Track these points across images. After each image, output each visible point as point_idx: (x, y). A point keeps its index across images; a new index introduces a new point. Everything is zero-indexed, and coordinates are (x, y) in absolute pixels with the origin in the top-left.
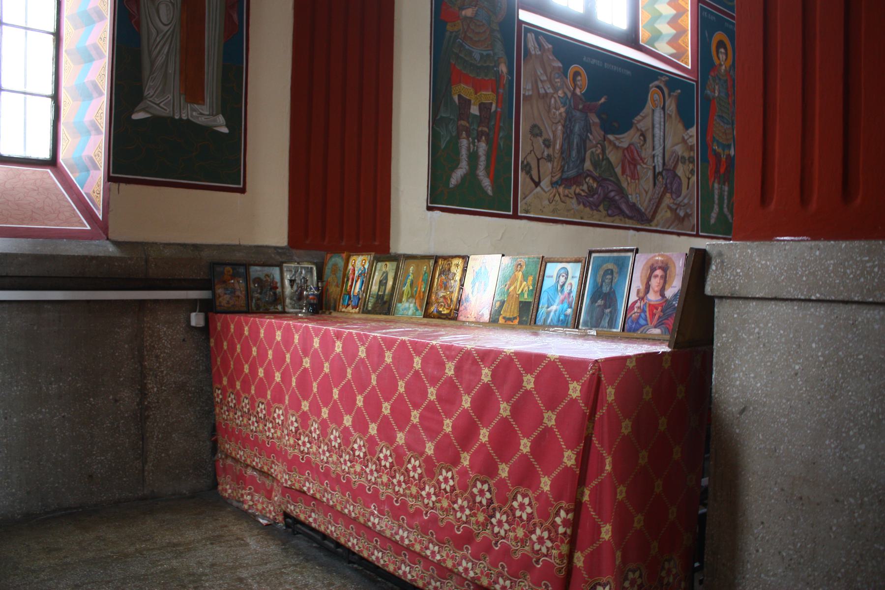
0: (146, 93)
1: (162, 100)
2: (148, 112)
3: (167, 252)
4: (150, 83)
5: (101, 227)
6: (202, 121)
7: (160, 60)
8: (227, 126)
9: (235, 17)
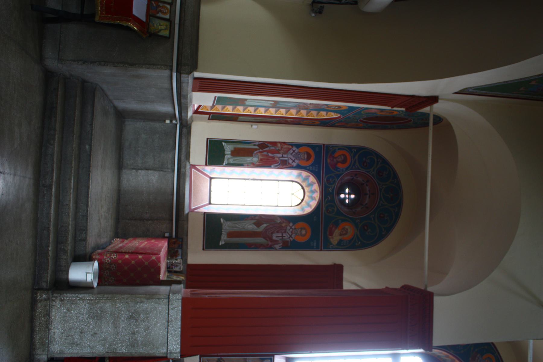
1: (227, 226)
5: (192, 211)
6: (222, 237)
7: (237, 226)
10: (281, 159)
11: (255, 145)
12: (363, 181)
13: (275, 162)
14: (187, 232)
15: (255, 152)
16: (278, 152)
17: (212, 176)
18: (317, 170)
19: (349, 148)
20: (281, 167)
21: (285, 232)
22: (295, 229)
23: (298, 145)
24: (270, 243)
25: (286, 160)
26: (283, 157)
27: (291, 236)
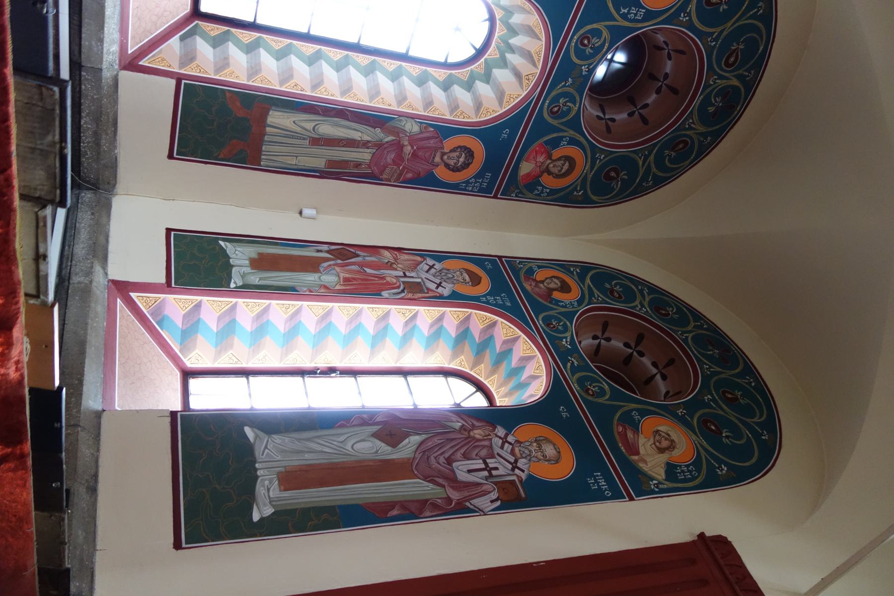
0: (274, 436)
1: (271, 455)
2: (255, 439)
3: (85, 451)
4: (287, 440)
6: (260, 490)
7: (313, 445)
8: (262, 519)
9: (395, 512)
10: (402, 279)
11: (318, 251)
12: (626, 345)
13: (390, 286)
14: (96, 476)
15: (326, 264)
16: (390, 266)
17: (191, 362)
18: (509, 304)
19: (564, 266)
20: (410, 296)
21: (493, 457)
22: (517, 441)
23: (440, 256)
24: (455, 496)
25: (419, 283)
26: (405, 276)
27: (515, 466)
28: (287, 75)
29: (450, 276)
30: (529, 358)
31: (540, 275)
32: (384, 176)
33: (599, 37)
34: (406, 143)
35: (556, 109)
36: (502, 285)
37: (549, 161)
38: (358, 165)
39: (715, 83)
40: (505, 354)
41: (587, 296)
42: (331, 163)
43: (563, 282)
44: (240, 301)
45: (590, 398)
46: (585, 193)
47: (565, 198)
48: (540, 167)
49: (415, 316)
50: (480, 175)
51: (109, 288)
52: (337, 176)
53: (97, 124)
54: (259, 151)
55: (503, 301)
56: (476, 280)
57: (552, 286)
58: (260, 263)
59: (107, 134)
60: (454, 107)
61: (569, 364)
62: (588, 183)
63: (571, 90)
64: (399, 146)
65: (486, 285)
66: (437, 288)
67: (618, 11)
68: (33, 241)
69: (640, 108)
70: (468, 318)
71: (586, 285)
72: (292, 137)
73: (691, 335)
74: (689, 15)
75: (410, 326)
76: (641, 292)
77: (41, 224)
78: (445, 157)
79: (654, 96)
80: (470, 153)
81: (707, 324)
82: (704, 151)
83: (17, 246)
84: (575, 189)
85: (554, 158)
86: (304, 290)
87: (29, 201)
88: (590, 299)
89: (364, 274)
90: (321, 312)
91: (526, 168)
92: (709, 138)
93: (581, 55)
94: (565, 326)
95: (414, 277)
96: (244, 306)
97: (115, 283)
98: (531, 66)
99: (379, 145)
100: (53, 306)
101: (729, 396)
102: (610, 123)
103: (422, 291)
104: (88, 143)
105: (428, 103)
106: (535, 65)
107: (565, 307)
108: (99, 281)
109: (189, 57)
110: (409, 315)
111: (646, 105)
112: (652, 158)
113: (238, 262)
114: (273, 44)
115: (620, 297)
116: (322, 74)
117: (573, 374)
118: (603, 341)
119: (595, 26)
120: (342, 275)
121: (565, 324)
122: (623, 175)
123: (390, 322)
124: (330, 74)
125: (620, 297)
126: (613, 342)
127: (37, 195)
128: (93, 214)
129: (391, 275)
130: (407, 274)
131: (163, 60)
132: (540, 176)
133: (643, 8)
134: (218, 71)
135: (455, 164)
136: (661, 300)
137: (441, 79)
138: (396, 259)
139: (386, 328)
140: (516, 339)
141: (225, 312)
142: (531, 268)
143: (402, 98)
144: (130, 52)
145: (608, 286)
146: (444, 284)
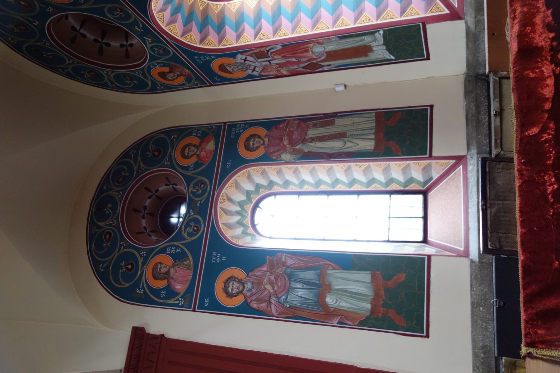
11: (329, 65)
12: (109, 45)
13: (278, 53)
15: (323, 58)
16: (281, 65)
20: (263, 49)
23: (250, 78)
25: (259, 58)
26: (269, 61)
28: (366, 171)
29: (240, 67)
30: (169, 24)
31: (181, 80)
32: (297, 122)
33: (188, 233)
34: (288, 146)
35: (202, 186)
36: (206, 68)
37: (198, 153)
38: (315, 126)
39: (113, 221)
40: (188, 22)
41: (146, 72)
42: (331, 123)
43: (165, 78)
44: (375, 22)
45: (117, 6)
46: (170, 137)
47: (182, 132)
48: (202, 149)
49: (256, 35)
50: (238, 135)
51: (464, 14)
52: (327, 116)
53: (478, 119)
54: (377, 122)
55: (200, 59)
56: (222, 68)
57: (171, 75)
58: (366, 50)
59: (472, 114)
60: (264, 173)
61: (141, 26)
62: (169, 144)
63: (196, 199)
64: (292, 143)
65: (215, 65)
66: (246, 58)
67: (182, 249)
68: (504, 126)
69: (152, 196)
70: (220, 41)
71: (149, 80)
72: (358, 135)
73: (67, 62)
74: (141, 256)
75: (257, 27)
76: (112, 83)
77: (498, 141)
78: (262, 142)
79: (147, 204)
80: (247, 148)
81: (60, 72)
82: (106, 179)
83: (515, 122)
84: (177, 139)
85: (195, 156)
86: (333, 38)
87: (507, 158)
88: (144, 72)
89: (296, 57)
90: (319, 25)
91: (211, 146)
92: (105, 188)
93: (196, 221)
94: (154, 51)
95: (263, 62)
96: (372, 19)
97: (460, 18)
98: (224, 207)
99: (304, 141)
100: (490, 72)
101: (22, 28)
102: (168, 183)
103: (255, 53)
104: (483, 106)
105: (279, 172)
106: (222, 209)
107: (158, 63)
108: (470, 18)
109: (426, 169)
110: (260, 35)
111: (149, 198)
112: (136, 169)
113: (380, 48)
114: (378, 186)
115: (124, 77)
116: (346, 176)
117: (135, 19)
118: (125, 44)
119: (193, 238)
120: (311, 53)
121: (154, 52)
122: (150, 154)
123: (272, 28)
124: (342, 177)
125: (124, 77)
126: (118, 44)
127: (502, 163)
128: (478, 60)
129: (279, 60)
130: (268, 63)
131: (441, 165)
132: (200, 143)
133: (168, 254)
134: (408, 165)
135: (255, 139)
136: (97, 80)
137: (275, 187)
138: (278, 70)
139: (273, 23)
140: (183, 35)
141: (384, 12)
142: (189, 83)
143: (296, 172)
144: (461, 167)
145: (135, 82)
146: (242, 61)
